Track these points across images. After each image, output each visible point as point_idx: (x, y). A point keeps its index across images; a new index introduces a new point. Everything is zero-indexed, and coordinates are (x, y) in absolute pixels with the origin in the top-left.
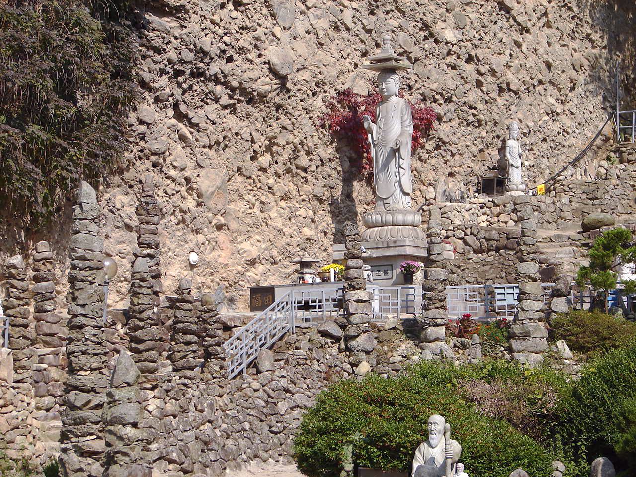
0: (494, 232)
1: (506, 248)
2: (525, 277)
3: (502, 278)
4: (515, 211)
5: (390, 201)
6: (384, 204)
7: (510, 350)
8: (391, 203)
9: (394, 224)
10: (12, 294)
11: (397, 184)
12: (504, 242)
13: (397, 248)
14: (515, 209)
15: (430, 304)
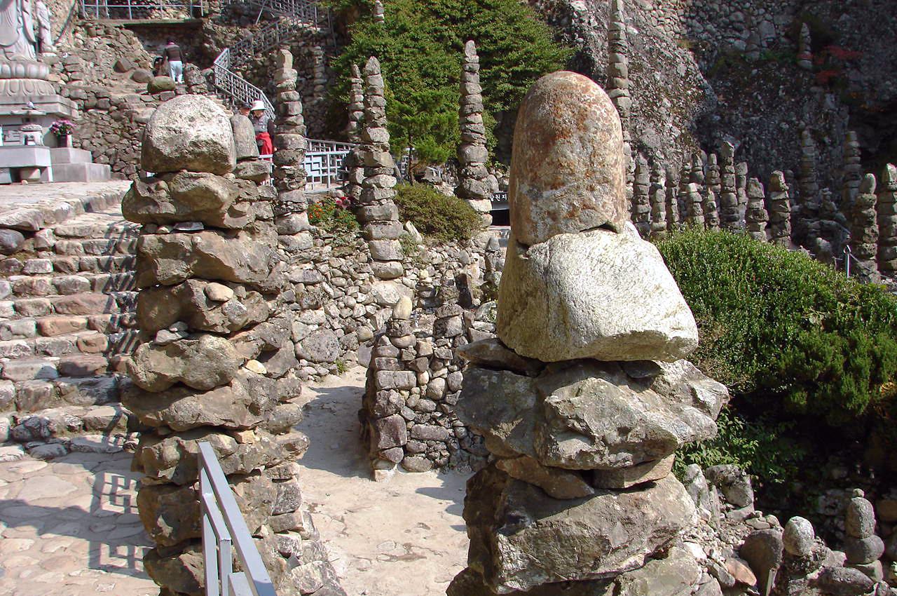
0: (80, 91)
1: (96, 107)
2: (378, 147)
3: (99, 138)
4: (65, 71)
5: (13, 49)
6: (5, 52)
7: (368, 237)
8: (14, 51)
9: (26, 77)
10: (214, 317)
11: (21, 30)
12: (94, 101)
13: (45, 105)
14: (65, 69)
15: (292, 183)
